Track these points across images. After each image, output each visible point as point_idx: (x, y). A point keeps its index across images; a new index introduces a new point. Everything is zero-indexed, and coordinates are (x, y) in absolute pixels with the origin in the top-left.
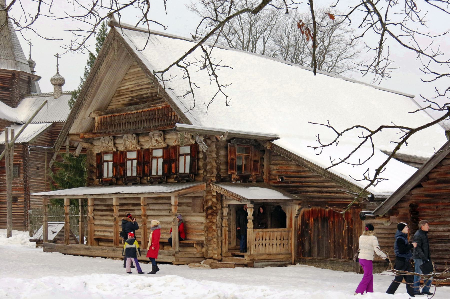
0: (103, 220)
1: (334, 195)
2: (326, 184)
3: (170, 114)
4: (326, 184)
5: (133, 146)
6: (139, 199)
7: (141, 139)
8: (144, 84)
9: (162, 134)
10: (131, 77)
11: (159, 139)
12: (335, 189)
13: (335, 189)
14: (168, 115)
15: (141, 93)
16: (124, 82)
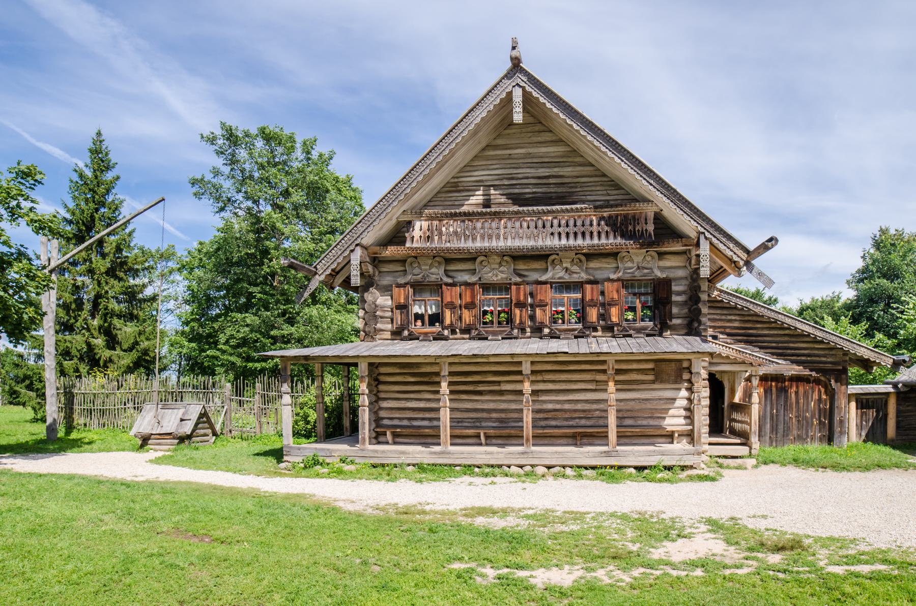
0: (406, 399)
1: (803, 358)
2: (792, 345)
3: (630, 228)
4: (792, 345)
5: (501, 276)
6: (604, 362)
7: (521, 266)
8: (527, 178)
9: (583, 258)
10: (490, 162)
11: (575, 268)
12: (806, 352)
13: (806, 352)
14: (627, 228)
15: (516, 191)
16: (468, 168)
